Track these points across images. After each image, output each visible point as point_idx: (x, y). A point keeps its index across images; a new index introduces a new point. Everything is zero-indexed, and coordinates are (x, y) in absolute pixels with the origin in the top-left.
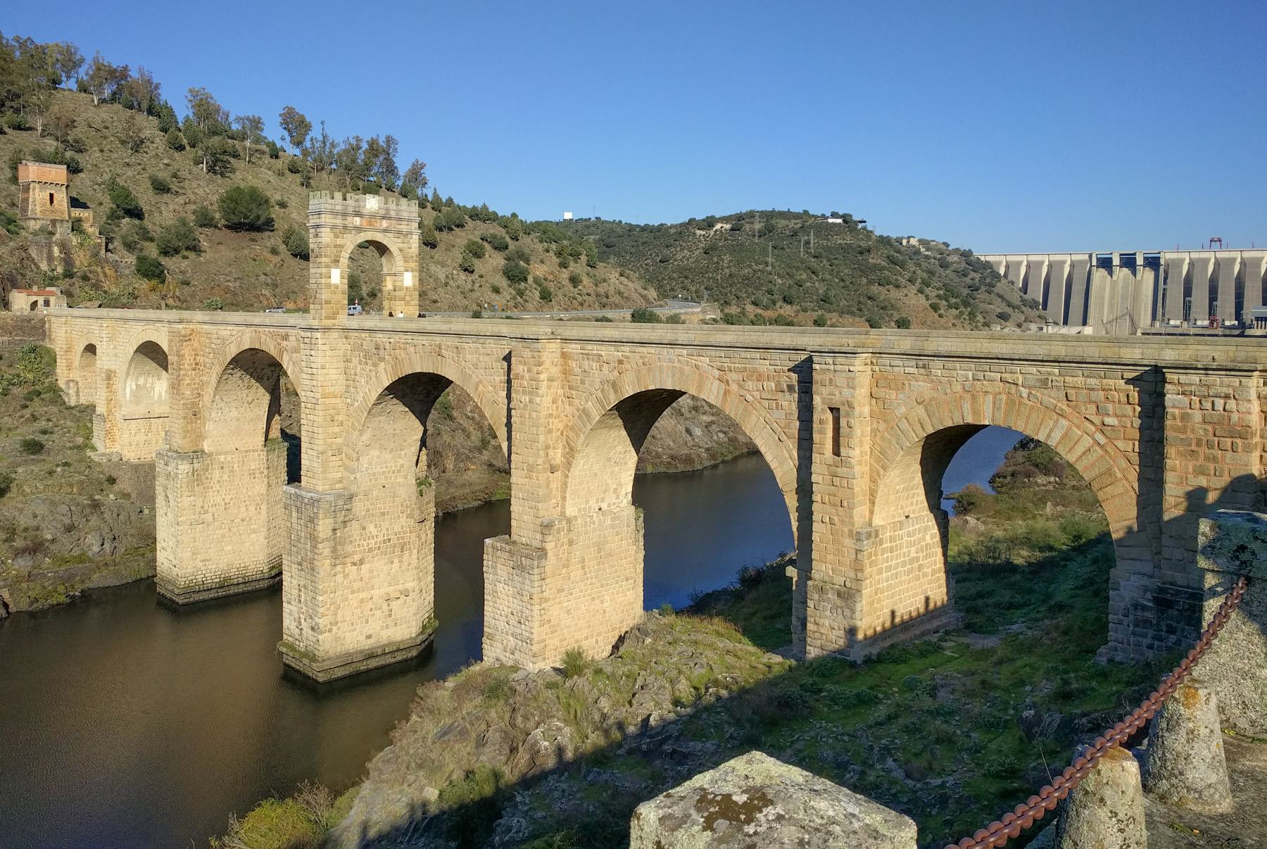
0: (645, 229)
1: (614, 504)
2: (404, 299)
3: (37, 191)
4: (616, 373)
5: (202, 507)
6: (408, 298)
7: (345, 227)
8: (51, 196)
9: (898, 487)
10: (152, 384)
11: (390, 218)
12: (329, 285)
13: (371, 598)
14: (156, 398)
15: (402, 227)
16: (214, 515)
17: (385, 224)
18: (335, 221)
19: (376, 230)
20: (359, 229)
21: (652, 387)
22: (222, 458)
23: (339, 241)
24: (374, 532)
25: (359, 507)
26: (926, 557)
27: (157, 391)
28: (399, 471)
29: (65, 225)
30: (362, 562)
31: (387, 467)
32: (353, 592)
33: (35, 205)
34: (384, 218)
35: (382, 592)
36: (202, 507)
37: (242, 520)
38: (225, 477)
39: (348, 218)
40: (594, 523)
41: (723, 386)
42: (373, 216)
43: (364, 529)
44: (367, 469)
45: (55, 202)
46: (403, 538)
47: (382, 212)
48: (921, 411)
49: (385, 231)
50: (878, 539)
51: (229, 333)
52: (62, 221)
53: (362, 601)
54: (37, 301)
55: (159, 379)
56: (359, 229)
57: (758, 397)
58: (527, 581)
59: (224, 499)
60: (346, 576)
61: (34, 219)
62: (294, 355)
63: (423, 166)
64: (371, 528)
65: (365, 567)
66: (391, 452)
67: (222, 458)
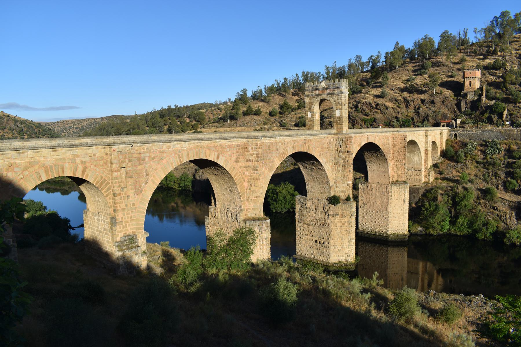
2: (336, 122)
7: (312, 95)
10: (413, 157)
11: (329, 89)
12: (307, 118)
14: (415, 163)
17: (328, 91)
19: (325, 94)
20: (317, 95)
23: (311, 101)
27: (415, 160)
29: (471, 93)
34: (327, 89)
39: (314, 91)
42: (323, 89)
47: (327, 86)
49: (328, 94)
52: (470, 92)
55: (415, 155)
56: (317, 95)
64: (312, 212)
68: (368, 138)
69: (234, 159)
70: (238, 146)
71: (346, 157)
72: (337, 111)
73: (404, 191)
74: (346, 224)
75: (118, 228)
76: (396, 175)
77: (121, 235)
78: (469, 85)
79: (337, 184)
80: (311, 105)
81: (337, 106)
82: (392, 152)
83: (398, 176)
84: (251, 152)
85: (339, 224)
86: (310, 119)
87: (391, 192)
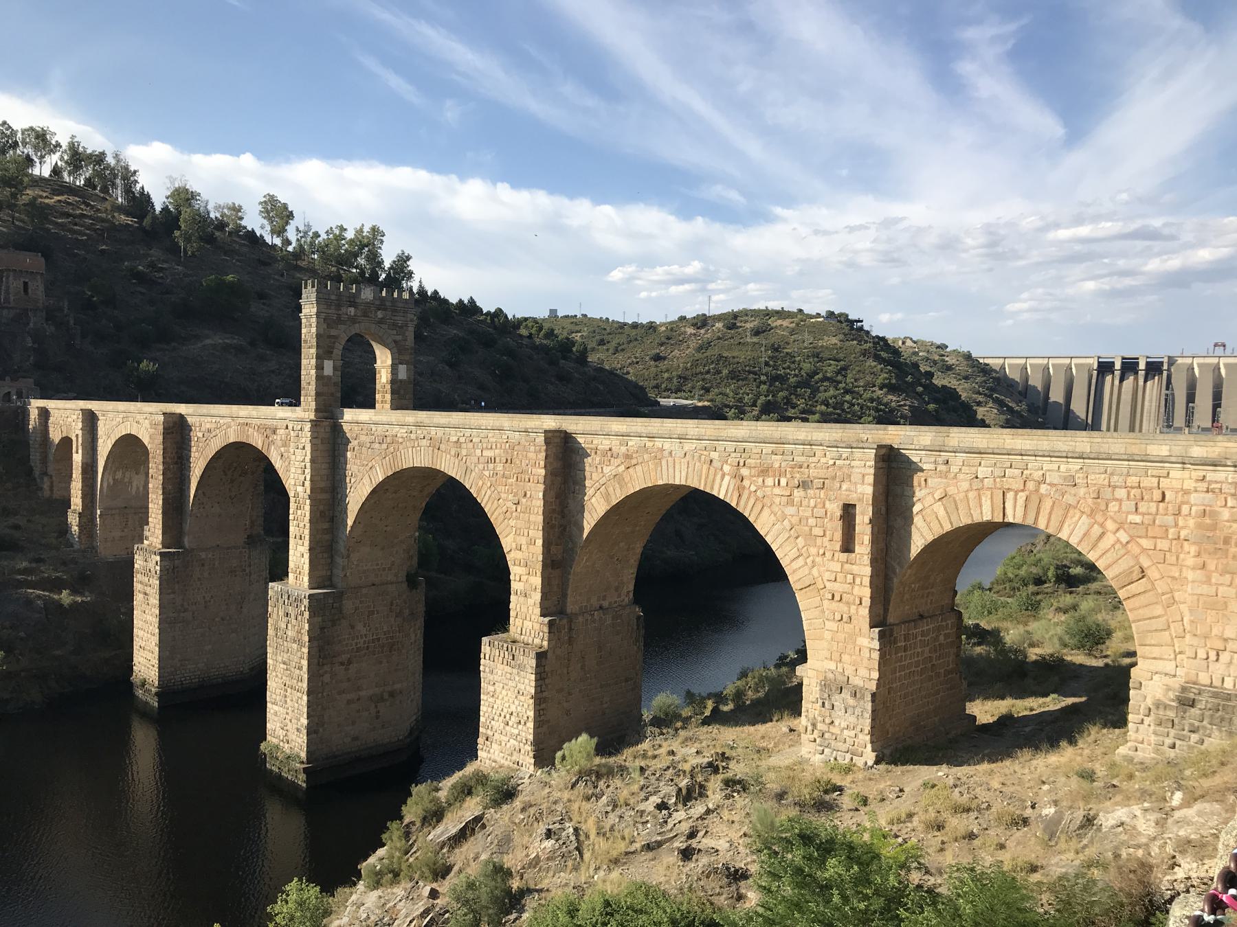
0: (635, 326)
1: (616, 602)
3: (11, 278)
4: (622, 468)
5: (182, 605)
6: (402, 392)
8: (26, 284)
9: (913, 586)
10: (130, 478)
11: (385, 309)
13: (358, 699)
15: (398, 318)
16: (193, 614)
17: (380, 314)
18: (330, 311)
20: (353, 320)
21: (660, 482)
22: (203, 555)
23: (333, 332)
24: (364, 631)
25: (348, 605)
26: (939, 658)
27: (134, 484)
28: (390, 569)
30: (350, 662)
31: (377, 565)
32: (339, 693)
33: (9, 294)
36: (182, 605)
37: (223, 619)
38: (206, 575)
40: (594, 621)
41: (733, 481)
43: (353, 627)
44: (357, 565)
45: (30, 290)
46: (392, 638)
47: (378, 302)
48: (939, 509)
50: (892, 638)
51: (214, 426)
53: (349, 702)
54: (9, 393)
56: (353, 320)
57: (770, 493)
58: (527, 681)
59: (204, 597)
61: (7, 308)
62: (282, 449)
63: (408, 258)
64: (360, 626)
66: (383, 549)
67: (203, 555)
72: (400, 366)
78: (22, 293)
80: (334, 343)
86: (329, 377)
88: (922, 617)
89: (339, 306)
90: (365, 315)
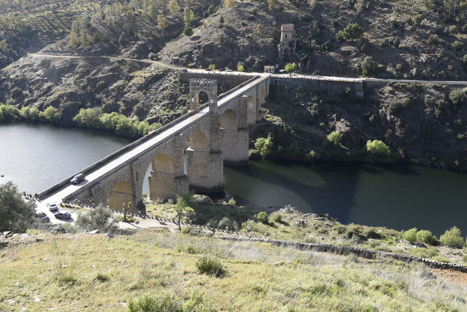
17: (205, 87)
20: (198, 89)
24: (198, 161)
35: (201, 175)
42: (202, 86)
49: (205, 89)
53: (196, 175)
56: (198, 89)
60: (192, 169)
64: (198, 160)
65: (196, 168)
67: (226, 131)
68: (226, 108)
69: (170, 149)
70: (171, 141)
71: (217, 127)
73: (246, 134)
74: (218, 165)
75: (137, 200)
76: (241, 124)
77: (137, 202)
79: (212, 143)
81: (211, 97)
82: (238, 110)
83: (242, 125)
84: (177, 143)
85: (214, 166)
86: (193, 102)
87: (238, 135)
88: (122, 193)
89: (195, 86)
90: (202, 87)
